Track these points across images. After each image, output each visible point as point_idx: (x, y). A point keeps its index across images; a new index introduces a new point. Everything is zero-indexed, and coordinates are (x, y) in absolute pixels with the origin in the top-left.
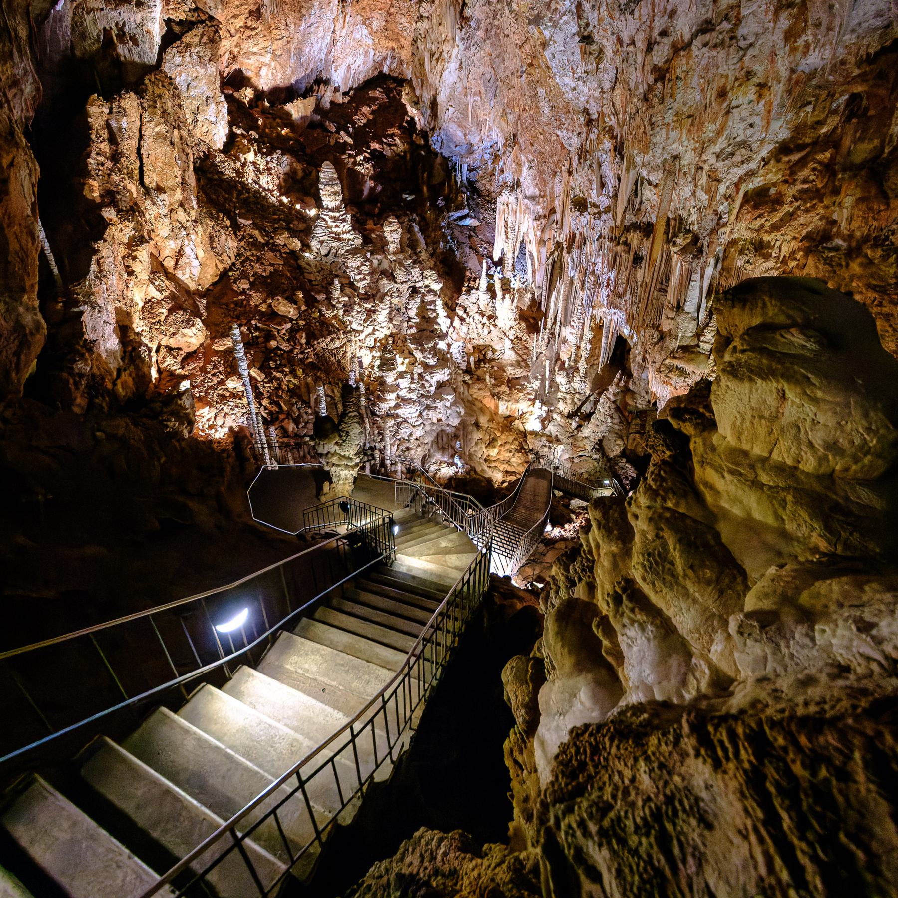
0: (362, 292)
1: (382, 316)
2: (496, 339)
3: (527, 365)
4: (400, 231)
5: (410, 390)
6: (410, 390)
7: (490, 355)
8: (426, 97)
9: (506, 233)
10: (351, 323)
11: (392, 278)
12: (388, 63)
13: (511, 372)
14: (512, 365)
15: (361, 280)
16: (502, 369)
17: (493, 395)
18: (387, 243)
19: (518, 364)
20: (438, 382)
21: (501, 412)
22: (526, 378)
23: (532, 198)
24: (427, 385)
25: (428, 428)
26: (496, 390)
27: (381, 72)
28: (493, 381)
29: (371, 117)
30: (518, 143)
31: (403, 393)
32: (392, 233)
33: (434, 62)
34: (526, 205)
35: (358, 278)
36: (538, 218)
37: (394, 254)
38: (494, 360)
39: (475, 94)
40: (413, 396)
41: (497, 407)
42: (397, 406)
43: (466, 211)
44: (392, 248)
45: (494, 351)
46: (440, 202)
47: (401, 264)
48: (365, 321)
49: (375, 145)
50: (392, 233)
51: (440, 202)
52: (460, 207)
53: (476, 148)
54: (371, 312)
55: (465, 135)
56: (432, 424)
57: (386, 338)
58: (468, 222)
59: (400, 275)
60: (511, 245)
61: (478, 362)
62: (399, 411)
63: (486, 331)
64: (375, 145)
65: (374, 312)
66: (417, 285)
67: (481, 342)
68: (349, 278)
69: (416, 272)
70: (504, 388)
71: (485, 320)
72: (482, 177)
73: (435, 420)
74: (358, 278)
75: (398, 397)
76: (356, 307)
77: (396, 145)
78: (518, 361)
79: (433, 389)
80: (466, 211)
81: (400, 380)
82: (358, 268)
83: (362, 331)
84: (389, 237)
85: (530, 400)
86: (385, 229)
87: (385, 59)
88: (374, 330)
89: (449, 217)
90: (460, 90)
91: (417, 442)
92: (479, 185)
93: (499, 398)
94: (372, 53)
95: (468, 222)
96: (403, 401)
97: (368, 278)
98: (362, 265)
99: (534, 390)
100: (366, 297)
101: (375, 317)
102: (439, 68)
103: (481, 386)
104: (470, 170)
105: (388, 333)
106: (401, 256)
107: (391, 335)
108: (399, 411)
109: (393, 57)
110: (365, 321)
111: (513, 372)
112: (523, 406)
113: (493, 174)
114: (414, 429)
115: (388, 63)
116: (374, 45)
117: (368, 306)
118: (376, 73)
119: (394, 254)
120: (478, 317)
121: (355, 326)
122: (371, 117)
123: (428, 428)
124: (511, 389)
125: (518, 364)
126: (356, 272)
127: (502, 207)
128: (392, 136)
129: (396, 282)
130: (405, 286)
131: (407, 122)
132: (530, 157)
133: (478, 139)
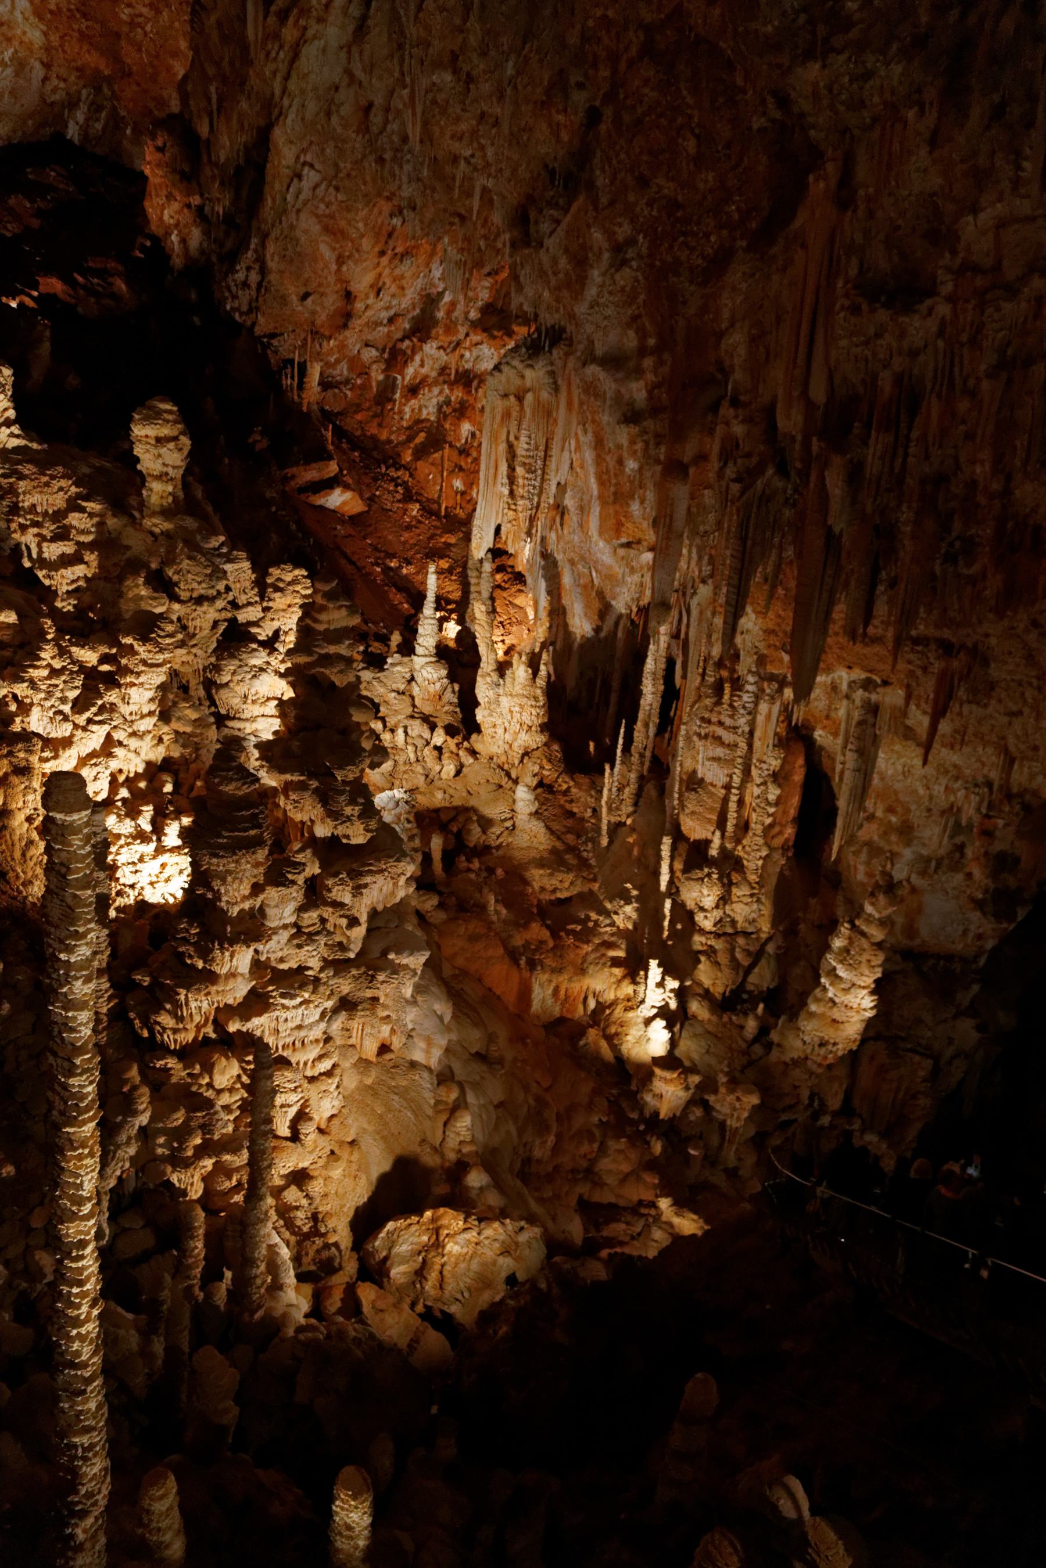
0: (66, 606)
1: (139, 696)
2: (484, 792)
3: (584, 863)
4: (186, 441)
5: (300, 935)
6: (300, 935)
7: (475, 835)
8: (228, 145)
9: (512, 479)
10: (25, 708)
11: (165, 587)
12: (80, 116)
13: (550, 884)
14: (541, 863)
15: (66, 561)
16: (516, 874)
17: (513, 956)
18: (140, 480)
19: (555, 860)
20: (374, 914)
21: (536, 1006)
22: (589, 900)
23: (613, 362)
24: (336, 920)
25: (351, 1081)
26: (518, 941)
27: (59, 135)
28: (504, 911)
29: (35, 223)
30: (591, 185)
31: (277, 948)
32: (158, 449)
33: (272, 20)
34: (591, 389)
35: (53, 551)
36: (631, 417)
37: (166, 513)
38: (487, 849)
39: (438, 65)
40: (311, 957)
41: (525, 994)
42: (256, 1002)
43: (333, 468)
44: (158, 492)
45: (486, 823)
46: (259, 441)
47: (194, 548)
48: (79, 705)
49: (54, 285)
50: (158, 449)
51: (259, 441)
52: (322, 455)
53: (359, 306)
54: (95, 684)
55: (340, 261)
56: (363, 1064)
57: (153, 771)
58: (336, 499)
59: (189, 577)
60: (523, 516)
61: (449, 857)
62: (259, 1024)
63: (450, 769)
64: (54, 285)
65: (111, 681)
66: (242, 617)
67: (438, 799)
68: (17, 551)
69: (240, 571)
70: (537, 931)
71: (439, 738)
72: (358, 408)
73: (370, 1048)
74: (53, 551)
75: (258, 966)
76: (47, 654)
77: (115, 296)
78: (553, 851)
79: (359, 932)
80: (333, 468)
81: (272, 893)
82: (58, 516)
83: (67, 742)
84: (148, 460)
85: (616, 962)
86: (138, 431)
87: (72, 104)
88: (109, 742)
89: (286, 479)
90: (346, 110)
91: (325, 1144)
92: (351, 423)
93: (532, 965)
94: (38, 71)
95: (336, 499)
96: (274, 982)
97: (91, 557)
98: (73, 506)
99: (621, 933)
100: (79, 628)
101: (112, 697)
102: (289, 34)
103: (474, 926)
104: (326, 384)
105: (157, 754)
106: (190, 523)
107: (167, 765)
108: (259, 1024)
109: (96, 108)
110: (79, 705)
111: (550, 883)
112: (603, 983)
113: (385, 395)
114: (312, 1092)
115: (80, 116)
116: (48, 49)
117: (89, 656)
118: (48, 131)
119: (166, 513)
120: (417, 728)
121: (37, 722)
122: (35, 223)
123: (351, 1081)
124: (555, 935)
125: (555, 860)
126: (47, 531)
127: (500, 405)
128: (102, 273)
129: (174, 598)
130: (209, 614)
131: (143, 248)
132: (624, 230)
133: (369, 278)
